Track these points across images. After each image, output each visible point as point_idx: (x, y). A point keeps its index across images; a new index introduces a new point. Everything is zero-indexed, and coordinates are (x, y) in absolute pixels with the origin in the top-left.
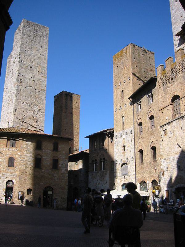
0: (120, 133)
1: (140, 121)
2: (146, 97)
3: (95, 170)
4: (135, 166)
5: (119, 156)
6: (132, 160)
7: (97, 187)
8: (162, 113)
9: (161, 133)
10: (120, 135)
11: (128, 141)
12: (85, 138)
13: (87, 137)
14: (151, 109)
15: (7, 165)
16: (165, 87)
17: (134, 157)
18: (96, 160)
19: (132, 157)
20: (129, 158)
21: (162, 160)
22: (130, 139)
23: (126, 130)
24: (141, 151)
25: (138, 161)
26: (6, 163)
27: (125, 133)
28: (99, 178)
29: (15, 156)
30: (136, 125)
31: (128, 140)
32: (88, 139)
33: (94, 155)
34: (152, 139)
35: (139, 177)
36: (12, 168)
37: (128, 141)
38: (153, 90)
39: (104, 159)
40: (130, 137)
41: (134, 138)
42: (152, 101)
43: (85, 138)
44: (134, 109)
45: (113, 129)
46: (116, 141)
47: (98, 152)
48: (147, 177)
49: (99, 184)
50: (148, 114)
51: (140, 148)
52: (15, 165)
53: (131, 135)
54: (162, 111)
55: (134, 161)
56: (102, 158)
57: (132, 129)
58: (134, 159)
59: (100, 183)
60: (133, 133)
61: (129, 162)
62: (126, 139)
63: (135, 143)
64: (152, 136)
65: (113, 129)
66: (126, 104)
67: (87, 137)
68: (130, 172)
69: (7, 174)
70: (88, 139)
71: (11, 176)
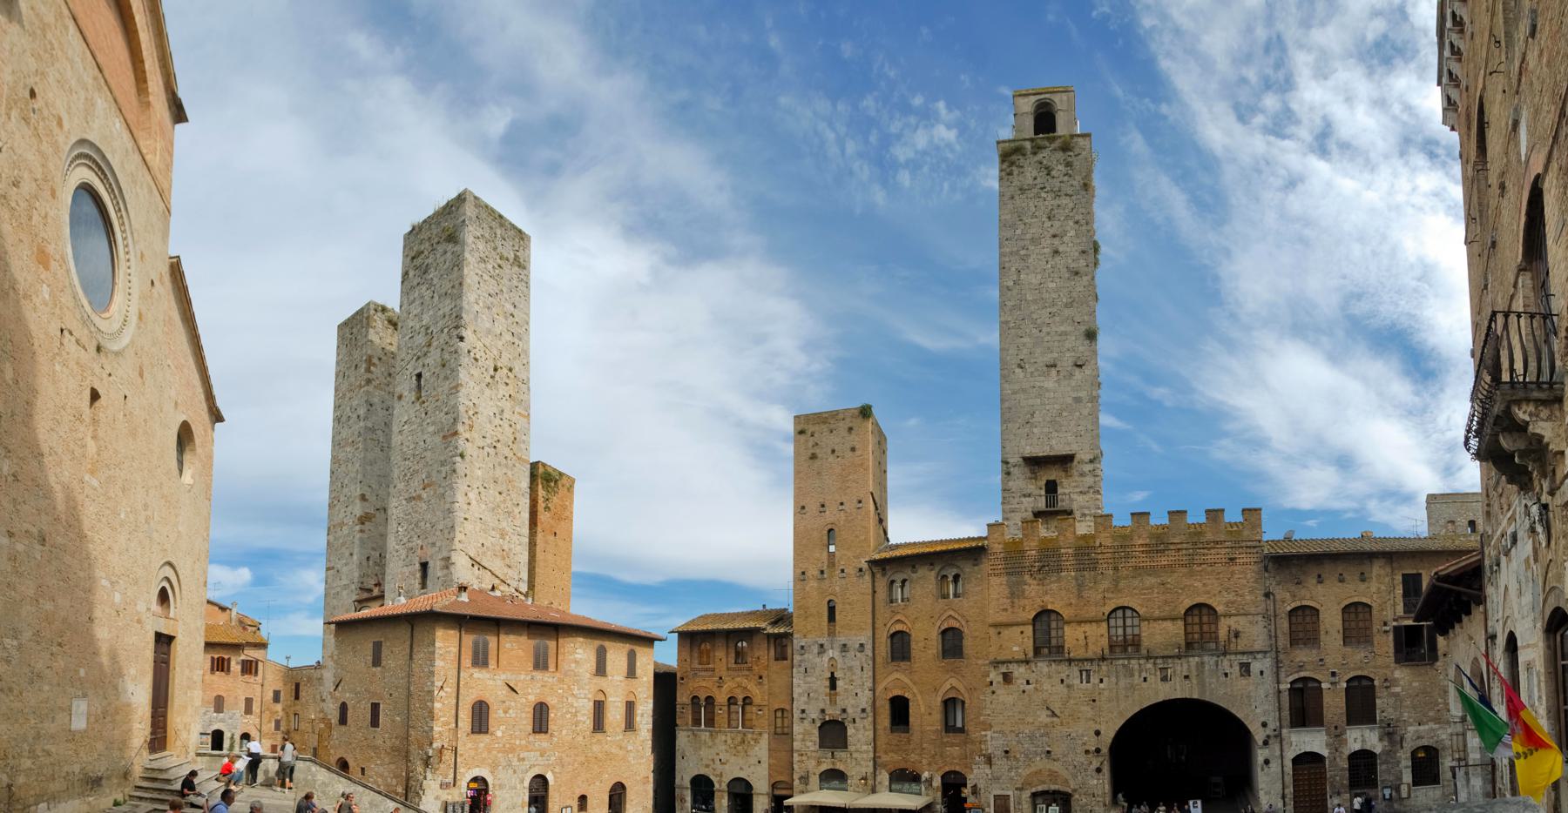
11: (850, 669)
15: (530, 728)
16: (1013, 578)
17: (869, 709)
19: (863, 710)
20: (850, 711)
21: (989, 733)
22: (856, 664)
23: (842, 639)
25: (885, 720)
26: (527, 722)
27: (837, 645)
29: (551, 701)
34: (954, 682)
35: (884, 758)
36: (542, 736)
37: (850, 669)
40: (857, 660)
52: (552, 726)
56: (740, 697)
62: (840, 661)
69: (532, 756)
71: (541, 761)
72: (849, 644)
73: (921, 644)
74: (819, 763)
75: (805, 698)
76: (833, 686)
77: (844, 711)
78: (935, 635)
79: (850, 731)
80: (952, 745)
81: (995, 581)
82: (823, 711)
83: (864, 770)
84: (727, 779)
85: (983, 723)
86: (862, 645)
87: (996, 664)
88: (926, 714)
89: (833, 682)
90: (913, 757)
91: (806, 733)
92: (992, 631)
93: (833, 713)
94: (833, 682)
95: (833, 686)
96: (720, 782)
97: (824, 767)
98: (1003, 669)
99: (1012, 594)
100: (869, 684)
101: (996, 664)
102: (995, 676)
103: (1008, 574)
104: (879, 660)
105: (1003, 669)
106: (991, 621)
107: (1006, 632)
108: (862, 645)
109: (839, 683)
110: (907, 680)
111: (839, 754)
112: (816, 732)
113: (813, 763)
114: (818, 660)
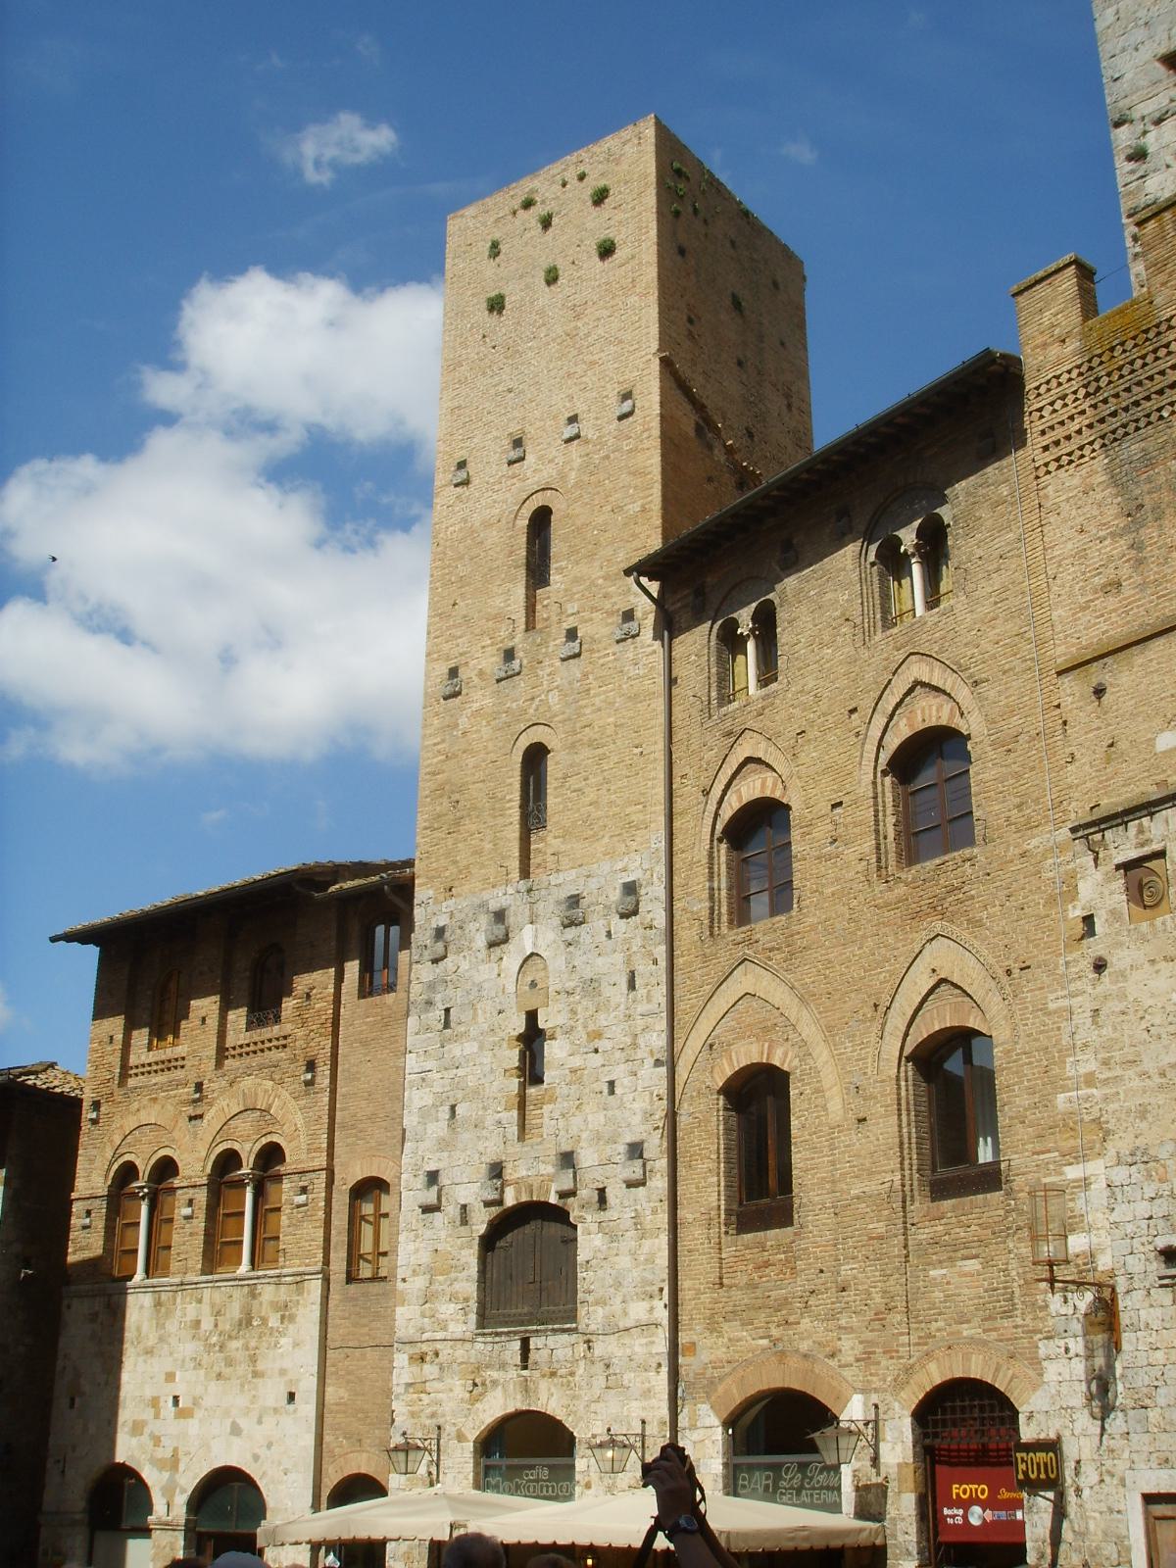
0: (494, 906)
1: (751, 788)
2: (847, 566)
3: (147, 1271)
4: (664, 1240)
5: (466, 1136)
6: (635, 1170)
7: (157, 1441)
8: (1099, 692)
9: (1072, 894)
10: (484, 920)
12: (69, 937)
13: (83, 937)
14: (918, 670)
16: (1132, 448)
17: (656, 1147)
18: (166, 1168)
19: (636, 1150)
20: (586, 1158)
21: (1096, 1168)
22: (610, 966)
24: (758, 1100)
25: (707, 1185)
27: (550, 908)
28: (189, 1348)
30: (698, 833)
31: (588, 974)
32: (92, 952)
33: (150, 1115)
34: (943, 957)
35: (706, 1351)
38: (960, 489)
39: (271, 1155)
40: (617, 950)
41: (661, 951)
42: (768, 671)
43: (69, 937)
44: (671, 682)
45: (410, 863)
46: (432, 986)
47: (199, 1087)
48: (849, 1347)
49: (183, 1414)
50: (880, 721)
51: (748, 1053)
53: (619, 926)
54: (1097, 674)
55: (659, 1183)
57: (644, 864)
58: (663, 1163)
59: (196, 1402)
60: (654, 911)
61: (586, 1193)
63: (681, 1006)
64: (938, 926)
65: (410, 863)
66: (572, 634)
67: (83, 937)
68: (601, 1302)
70: (92, 952)
72: (589, 889)
73: (822, 830)
74: (477, 1388)
75: (438, 1128)
76: (531, 1070)
77: (567, 1160)
78: (863, 775)
79: (589, 1243)
80: (954, 1251)
81: (1063, 485)
82: (497, 1171)
83: (635, 1410)
84: (190, 1479)
85: (1068, 1124)
86: (631, 889)
87: (1096, 827)
88: (851, 1129)
89: (532, 1038)
90: (809, 1332)
91: (439, 1266)
92: (1072, 691)
93: (533, 1175)
94: (532, 1038)
95: (531, 1070)
96: (169, 1490)
97: (495, 1407)
98: (1124, 845)
99: (1134, 512)
100: (658, 1040)
101: (1096, 827)
102: (1098, 889)
103: (1110, 441)
104: (686, 935)
105: (1124, 845)
106: (1062, 652)
107: (1125, 678)
108: (631, 889)
109: (554, 1051)
110: (776, 992)
111: (551, 1345)
112: (470, 1257)
113: (459, 1387)
114: (486, 972)
